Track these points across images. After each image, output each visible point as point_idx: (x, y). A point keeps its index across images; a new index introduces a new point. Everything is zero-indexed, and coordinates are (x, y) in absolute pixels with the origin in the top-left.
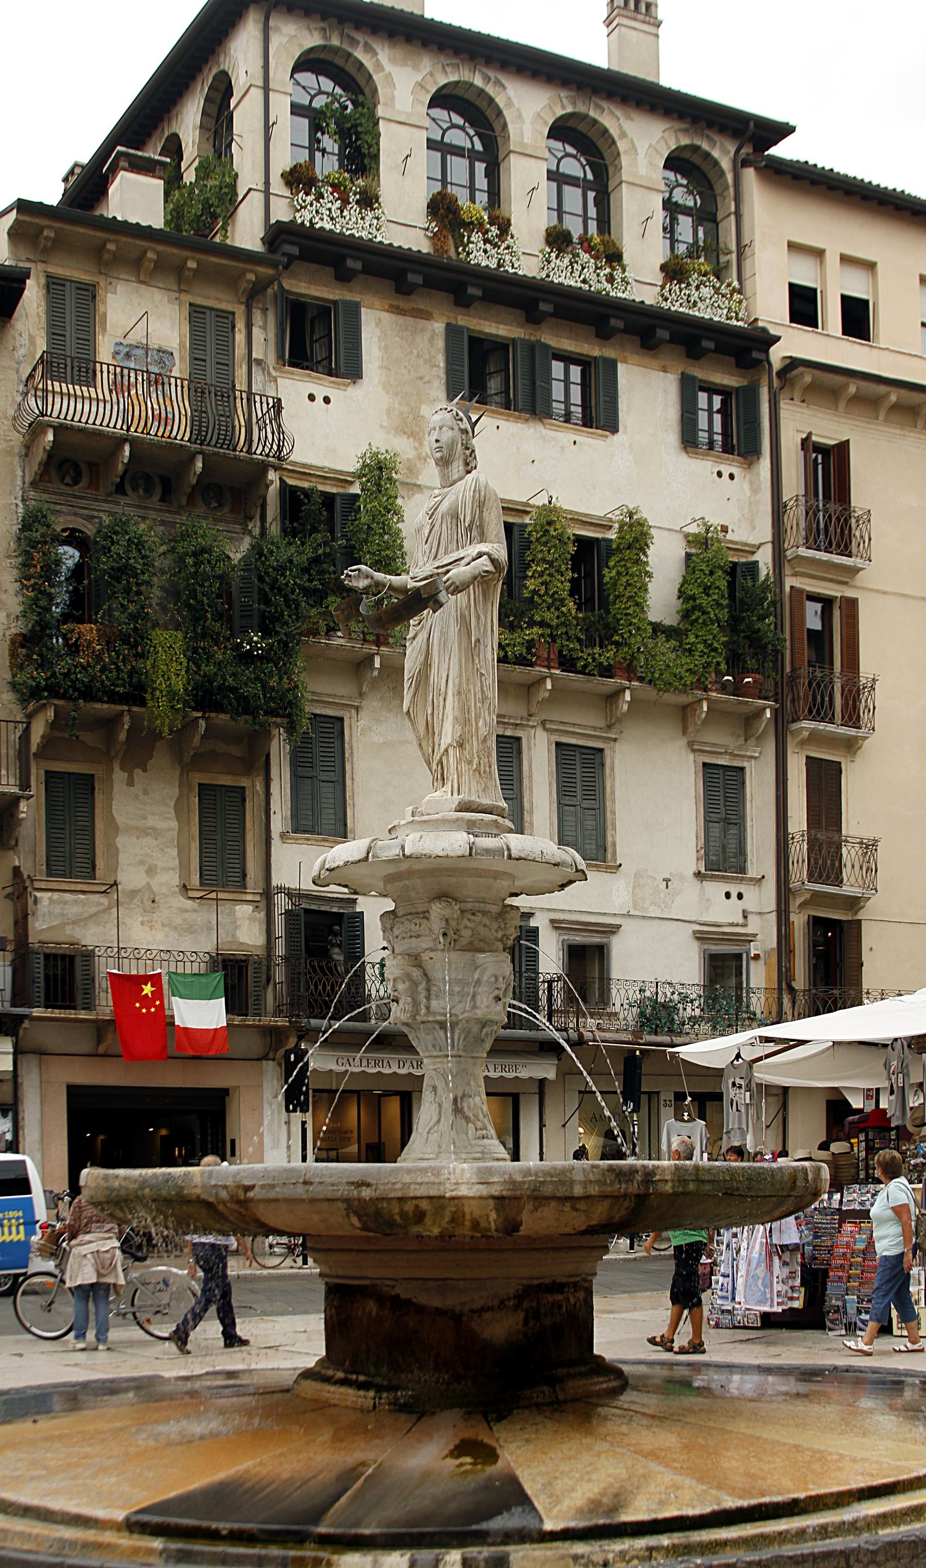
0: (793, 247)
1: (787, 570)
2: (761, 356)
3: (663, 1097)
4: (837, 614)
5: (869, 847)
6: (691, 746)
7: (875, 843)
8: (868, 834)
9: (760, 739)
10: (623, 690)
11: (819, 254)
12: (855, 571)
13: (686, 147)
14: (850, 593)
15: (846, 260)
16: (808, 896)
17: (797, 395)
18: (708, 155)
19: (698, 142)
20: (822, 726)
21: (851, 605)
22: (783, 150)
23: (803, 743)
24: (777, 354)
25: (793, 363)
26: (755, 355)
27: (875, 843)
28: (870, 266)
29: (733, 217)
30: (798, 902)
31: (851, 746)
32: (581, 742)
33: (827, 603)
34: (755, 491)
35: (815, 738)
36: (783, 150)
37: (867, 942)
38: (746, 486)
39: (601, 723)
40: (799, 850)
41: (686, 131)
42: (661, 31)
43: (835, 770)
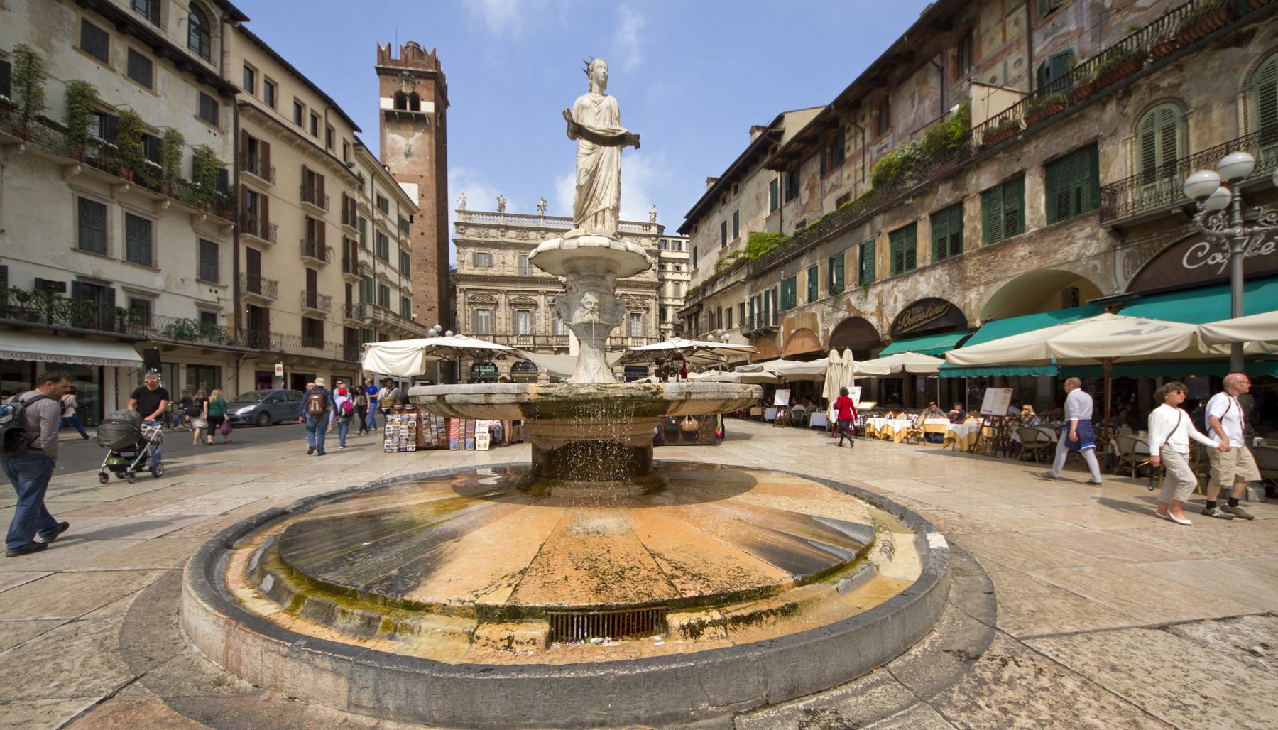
1: (240, 177)
3: (181, 365)
4: (259, 200)
5: (273, 284)
6: (195, 230)
7: (276, 283)
9: (225, 236)
10: (166, 200)
12: (269, 186)
14: (265, 194)
21: (265, 200)
23: (246, 241)
27: (276, 283)
31: (266, 247)
32: (140, 216)
33: (254, 195)
34: (226, 142)
35: (251, 241)
38: (221, 140)
39: (151, 210)
40: (244, 279)
43: (259, 254)
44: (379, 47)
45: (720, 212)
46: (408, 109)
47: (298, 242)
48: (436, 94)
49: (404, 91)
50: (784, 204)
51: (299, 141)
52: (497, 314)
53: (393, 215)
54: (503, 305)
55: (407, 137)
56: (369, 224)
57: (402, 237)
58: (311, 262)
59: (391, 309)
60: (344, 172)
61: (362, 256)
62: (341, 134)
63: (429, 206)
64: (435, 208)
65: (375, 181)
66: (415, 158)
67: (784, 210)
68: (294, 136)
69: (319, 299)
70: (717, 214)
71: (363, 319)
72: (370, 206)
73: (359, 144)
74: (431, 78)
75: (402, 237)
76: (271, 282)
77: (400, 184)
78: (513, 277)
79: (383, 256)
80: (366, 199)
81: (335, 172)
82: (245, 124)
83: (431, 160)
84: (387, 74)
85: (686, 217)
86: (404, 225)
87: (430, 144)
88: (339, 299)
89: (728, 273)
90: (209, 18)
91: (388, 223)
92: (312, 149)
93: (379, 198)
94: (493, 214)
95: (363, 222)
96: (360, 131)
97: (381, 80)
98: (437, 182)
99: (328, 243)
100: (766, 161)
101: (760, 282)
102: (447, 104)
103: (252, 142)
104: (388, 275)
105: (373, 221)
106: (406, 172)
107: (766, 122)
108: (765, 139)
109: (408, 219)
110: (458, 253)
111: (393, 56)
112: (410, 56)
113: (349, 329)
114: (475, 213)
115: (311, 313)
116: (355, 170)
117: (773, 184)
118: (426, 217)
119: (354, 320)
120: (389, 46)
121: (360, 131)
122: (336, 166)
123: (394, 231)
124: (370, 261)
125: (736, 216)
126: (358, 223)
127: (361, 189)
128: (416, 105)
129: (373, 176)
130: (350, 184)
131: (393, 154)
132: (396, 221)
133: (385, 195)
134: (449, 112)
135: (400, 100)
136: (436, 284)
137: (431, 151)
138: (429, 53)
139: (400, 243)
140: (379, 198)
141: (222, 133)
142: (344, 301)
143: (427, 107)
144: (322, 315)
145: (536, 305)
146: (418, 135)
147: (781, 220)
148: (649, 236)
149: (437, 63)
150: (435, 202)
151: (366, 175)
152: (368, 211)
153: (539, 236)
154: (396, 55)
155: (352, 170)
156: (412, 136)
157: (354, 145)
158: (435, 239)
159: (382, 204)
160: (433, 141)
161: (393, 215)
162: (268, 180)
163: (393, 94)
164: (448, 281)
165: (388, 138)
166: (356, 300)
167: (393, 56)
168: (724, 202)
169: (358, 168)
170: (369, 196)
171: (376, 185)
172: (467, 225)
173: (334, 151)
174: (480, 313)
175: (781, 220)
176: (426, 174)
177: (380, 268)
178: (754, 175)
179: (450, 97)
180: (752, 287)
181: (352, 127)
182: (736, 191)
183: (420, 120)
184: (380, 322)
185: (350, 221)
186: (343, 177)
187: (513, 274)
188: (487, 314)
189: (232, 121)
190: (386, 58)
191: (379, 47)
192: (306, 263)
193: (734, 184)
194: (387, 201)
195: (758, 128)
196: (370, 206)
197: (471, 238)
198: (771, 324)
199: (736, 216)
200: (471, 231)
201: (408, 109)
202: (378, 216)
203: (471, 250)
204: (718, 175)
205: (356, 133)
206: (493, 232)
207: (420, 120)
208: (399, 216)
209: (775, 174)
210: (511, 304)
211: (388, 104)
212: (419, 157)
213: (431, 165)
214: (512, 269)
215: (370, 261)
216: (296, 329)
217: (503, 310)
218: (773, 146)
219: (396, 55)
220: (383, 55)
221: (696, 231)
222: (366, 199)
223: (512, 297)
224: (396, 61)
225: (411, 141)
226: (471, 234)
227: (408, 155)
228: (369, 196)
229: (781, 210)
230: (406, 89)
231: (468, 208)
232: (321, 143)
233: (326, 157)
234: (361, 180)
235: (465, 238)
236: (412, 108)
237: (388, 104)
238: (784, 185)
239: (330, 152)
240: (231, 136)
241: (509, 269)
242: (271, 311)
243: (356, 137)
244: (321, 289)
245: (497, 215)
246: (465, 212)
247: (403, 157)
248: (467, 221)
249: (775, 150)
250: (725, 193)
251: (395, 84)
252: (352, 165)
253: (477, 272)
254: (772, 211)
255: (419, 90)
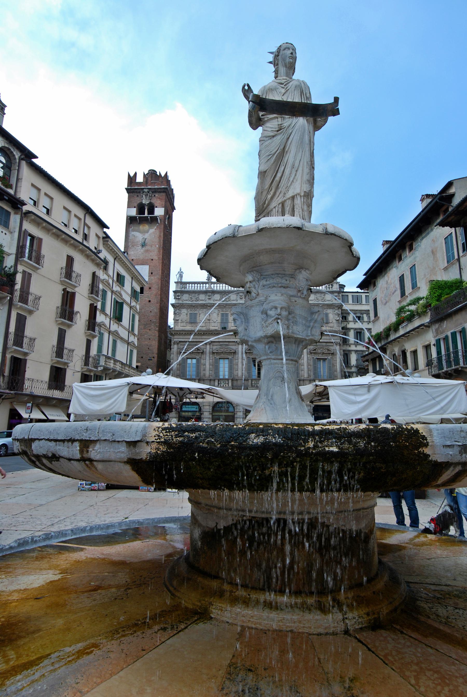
0: (33, 185)
2: (21, 207)
8: (33, 336)
11: (39, 190)
12: (38, 269)
13: (6, 147)
15: (46, 194)
16: (13, 350)
17: (29, 220)
18: (12, 152)
19: (10, 148)
20: (24, 305)
22: (34, 160)
24: (25, 208)
25: (29, 212)
26: (19, 206)
28: (52, 199)
29: (16, 171)
30: (9, 351)
36: (34, 160)
37: (28, 365)
41: (7, 143)
42: (5, 116)
44: (129, 175)
45: (397, 267)
46: (146, 214)
47: (55, 309)
48: (165, 202)
49: (144, 202)
50: (461, 254)
51: (64, 236)
52: (202, 361)
53: (128, 287)
54: (208, 354)
55: (144, 232)
56: (109, 294)
57: (133, 304)
58: (63, 323)
59: (117, 358)
60: (94, 256)
61: (100, 318)
62: (94, 229)
63: (156, 278)
64: (160, 282)
65: (116, 262)
66: (148, 248)
67: (462, 260)
68: (60, 233)
69: (65, 351)
70: (394, 269)
71: (96, 367)
72: (111, 281)
73: (107, 237)
74: (164, 192)
75: (133, 304)
76: (31, 339)
77: (136, 267)
78: (216, 330)
79: (118, 318)
80: (109, 276)
81: (88, 257)
82: (28, 226)
83: (159, 248)
84: (133, 192)
85: (364, 275)
86: (134, 294)
87: (160, 236)
88: (80, 352)
89: (410, 318)
90: (12, 158)
91: (123, 293)
92: (72, 242)
93: (118, 275)
94: (203, 283)
95: (104, 292)
96: (108, 228)
97: (129, 198)
98: (163, 263)
99: (76, 309)
100: (438, 221)
101: (445, 324)
102: (173, 208)
103: (33, 238)
104: (120, 332)
105: (112, 292)
106: (141, 257)
107: (435, 190)
108: (436, 202)
109: (139, 290)
110: (175, 314)
111: (138, 180)
112: (150, 179)
113: (85, 375)
114: (189, 283)
115: (58, 362)
116: (102, 255)
117: (448, 239)
118: (153, 288)
119: (90, 367)
120: (136, 174)
121: (108, 228)
122: (88, 252)
123: (127, 298)
124: (107, 322)
125: (413, 269)
126: (100, 293)
127: (105, 268)
128: (151, 211)
129: (115, 259)
130: (98, 265)
131: (133, 246)
132: (130, 293)
133: (123, 272)
134: (175, 214)
135: (141, 209)
136: (157, 339)
137: (160, 242)
138: (163, 175)
139: (131, 308)
140: (118, 275)
141: (11, 233)
142: (84, 353)
143: (159, 212)
144: (66, 364)
145: (235, 353)
146: (152, 231)
147: (460, 269)
148: (332, 292)
149: (168, 182)
150: (160, 277)
151: (110, 259)
152: (109, 284)
153: (239, 297)
154: (140, 179)
155: (99, 255)
156: (147, 232)
157: (103, 238)
158: (159, 304)
159: (120, 279)
160: (162, 234)
161: (128, 287)
162: (38, 264)
163: (136, 205)
164: (166, 337)
165: (130, 235)
166: (94, 351)
167: (138, 180)
168: (400, 259)
169: (104, 254)
170: (111, 273)
171: (117, 265)
172: (182, 292)
173: (88, 242)
174: (189, 361)
175: (460, 269)
176: (155, 258)
177: (114, 327)
178: (428, 234)
179: (176, 204)
180: (437, 330)
181: (103, 225)
182: (411, 249)
183: (154, 220)
184: (110, 369)
185: (95, 292)
186: (93, 261)
187: (217, 328)
188: (194, 361)
189: (18, 224)
190: (133, 181)
191: (129, 175)
192: (59, 324)
193: (408, 243)
194: (124, 277)
195: (428, 196)
196: (111, 281)
197: (185, 302)
198: (462, 364)
199: (413, 269)
200: (186, 297)
201: (146, 214)
202: (116, 288)
203: (184, 311)
204: (393, 238)
205: (105, 230)
206: (202, 297)
207: (154, 220)
208: (132, 288)
209: (447, 230)
210: (214, 353)
211: (134, 212)
212: (151, 246)
213: (159, 251)
214: (216, 324)
215: (107, 322)
216: (46, 375)
217: (208, 358)
218: (444, 208)
219: (140, 179)
220: (132, 179)
221: (375, 285)
222: (109, 276)
223: (215, 347)
224: (140, 183)
225: (146, 236)
226: (185, 298)
227: (143, 245)
228: (111, 273)
229: (459, 260)
230: (145, 201)
231: (184, 280)
232: (79, 238)
233: (81, 247)
234: (106, 262)
235: (181, 302)
236: (148, 214)
237: (134, 212)
238: (460, 238)
239: (85, 243)
240: (16, 235)
241: (213, 324)
242: (28, 361)
243: (105, 233)
244: (68, 344)
245: (206, 283)
246: (181, 283)
247: (140, 247)
248: (183, 289)
249: (447, 209)
250: (401, 251)
251: (138, 199)
252: (100, 252)
253: (188, 328)
254: (448, 262)
255: (153, 201)
